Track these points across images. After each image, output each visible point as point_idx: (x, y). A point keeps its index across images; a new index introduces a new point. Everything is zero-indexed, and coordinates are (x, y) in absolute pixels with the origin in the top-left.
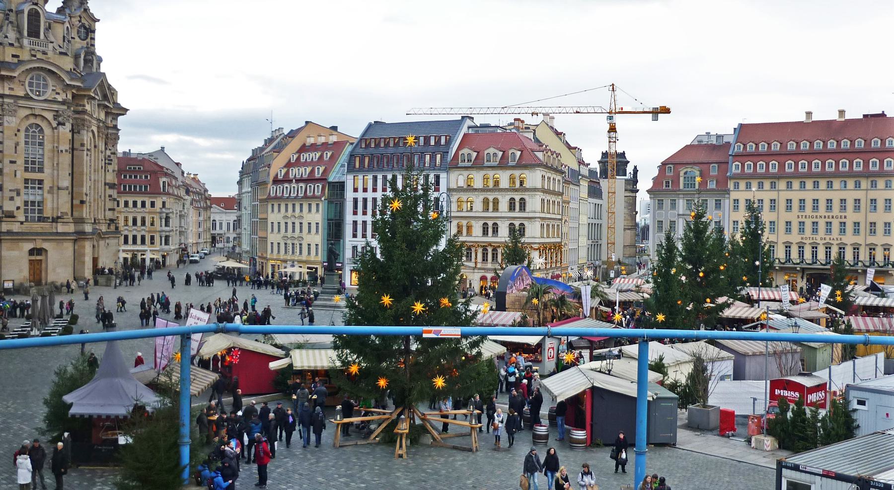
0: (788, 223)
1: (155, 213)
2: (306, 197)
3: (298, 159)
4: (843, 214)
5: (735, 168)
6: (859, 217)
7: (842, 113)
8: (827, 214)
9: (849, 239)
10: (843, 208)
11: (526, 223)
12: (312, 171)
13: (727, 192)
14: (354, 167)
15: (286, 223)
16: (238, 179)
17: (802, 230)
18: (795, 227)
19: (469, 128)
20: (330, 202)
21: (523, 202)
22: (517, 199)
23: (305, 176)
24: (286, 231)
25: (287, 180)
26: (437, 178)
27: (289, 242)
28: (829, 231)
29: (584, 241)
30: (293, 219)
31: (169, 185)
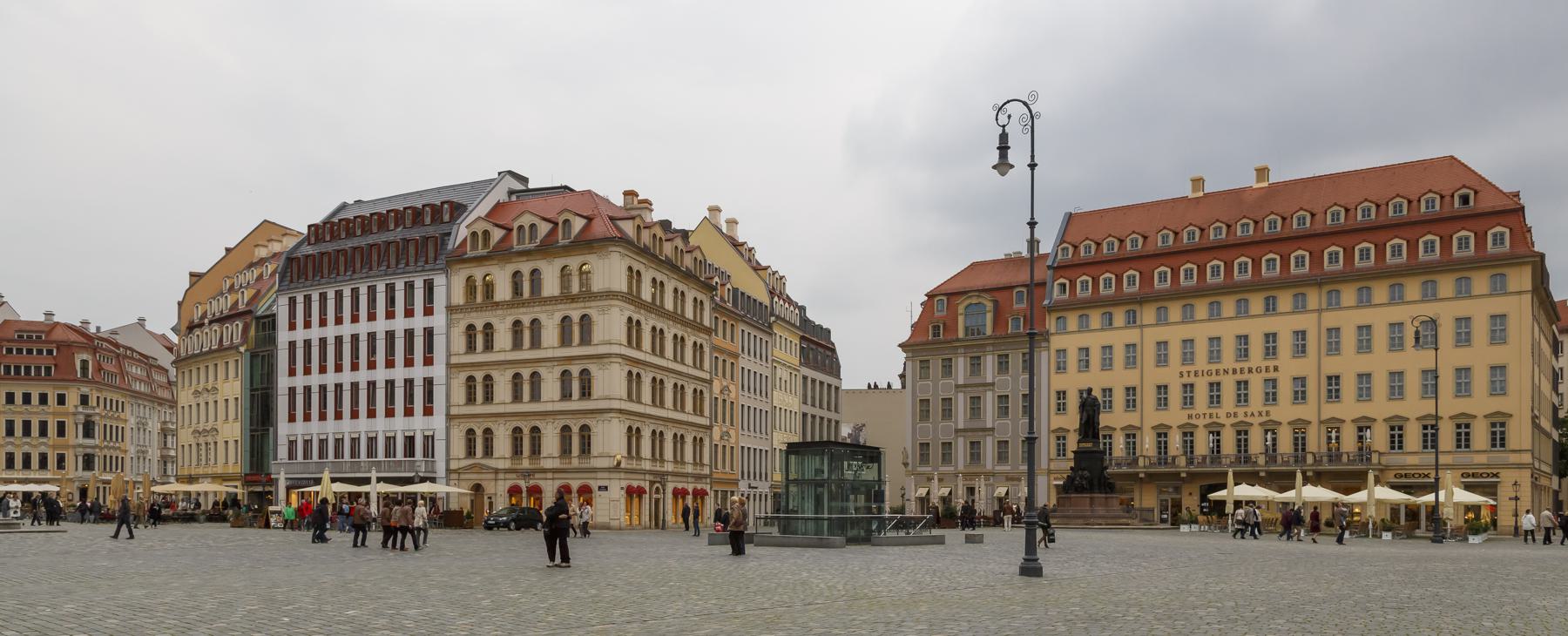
0: (1162, 389)
1: (67, 414)
2: (221, 349)
4: (1271, 364)
6: (1305, 367)
8: (1238, 366)
9: (1285, 411)
10: (1271, 351)
11: (593, 368)
13: (1046, 336)
17: (1188, 401)
18: (1175, 395)
21: (585, 320)
22: (576, 316)
26: (429, 288)
27: (202, 440)
28: (1242, 398)
31: (99, 369)
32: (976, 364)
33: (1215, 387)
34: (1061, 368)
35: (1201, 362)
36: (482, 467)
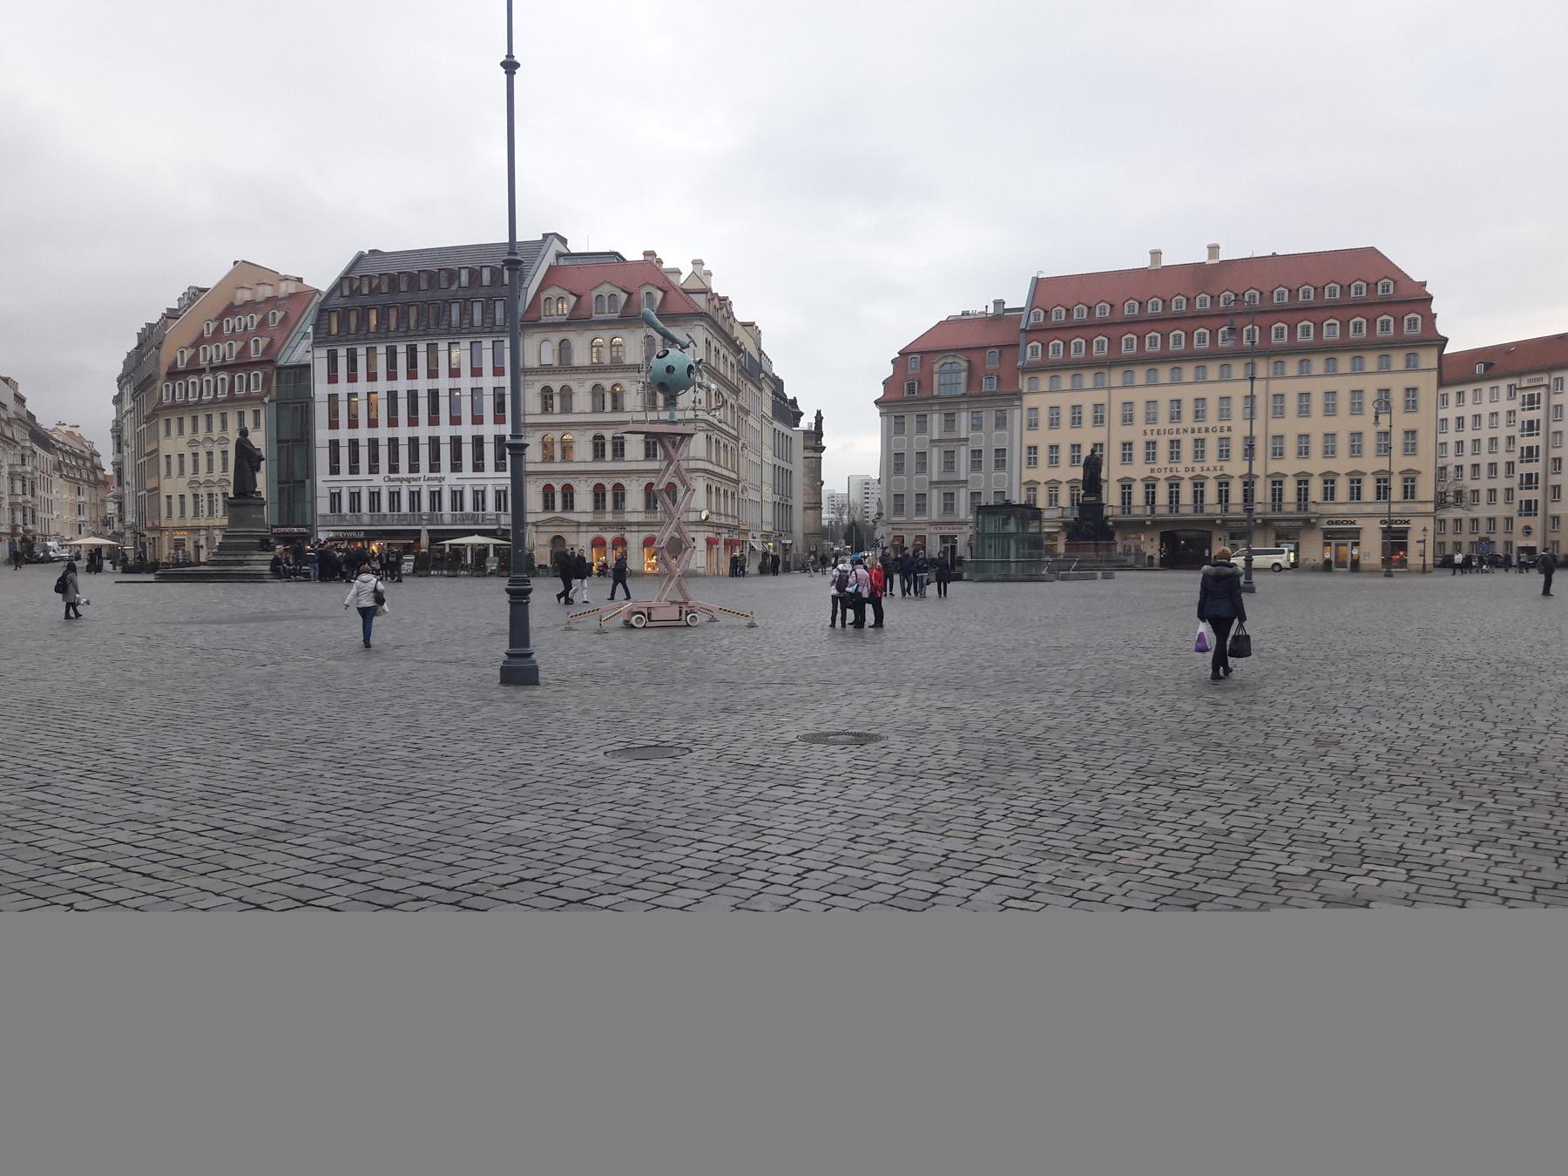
0: (1127, 445)
2: (232, 399)
3: (219, 329)
4: (1225, 424)
5: (1031, 352)
7: (1214, 249)
8: (1196, 426)
12: (245, 348)
13: (1018, 395)
14: (329, 333)
15: (195, 455)
16: (117, 392)
17: (1151, 456)
18: (1139, 452)
19: (559, 255)
20: (280, 404)
23: (230, 360)
24: (196, 471)
25: (194, 370)
27: (202, 491)
28: (1199, 454)
29: (768, 495)
30: (208, 445)
32: (950, 421)
33: (1175, 444)
34: (1033, 425)
35: (1163, 421)
36: (562, 520)
